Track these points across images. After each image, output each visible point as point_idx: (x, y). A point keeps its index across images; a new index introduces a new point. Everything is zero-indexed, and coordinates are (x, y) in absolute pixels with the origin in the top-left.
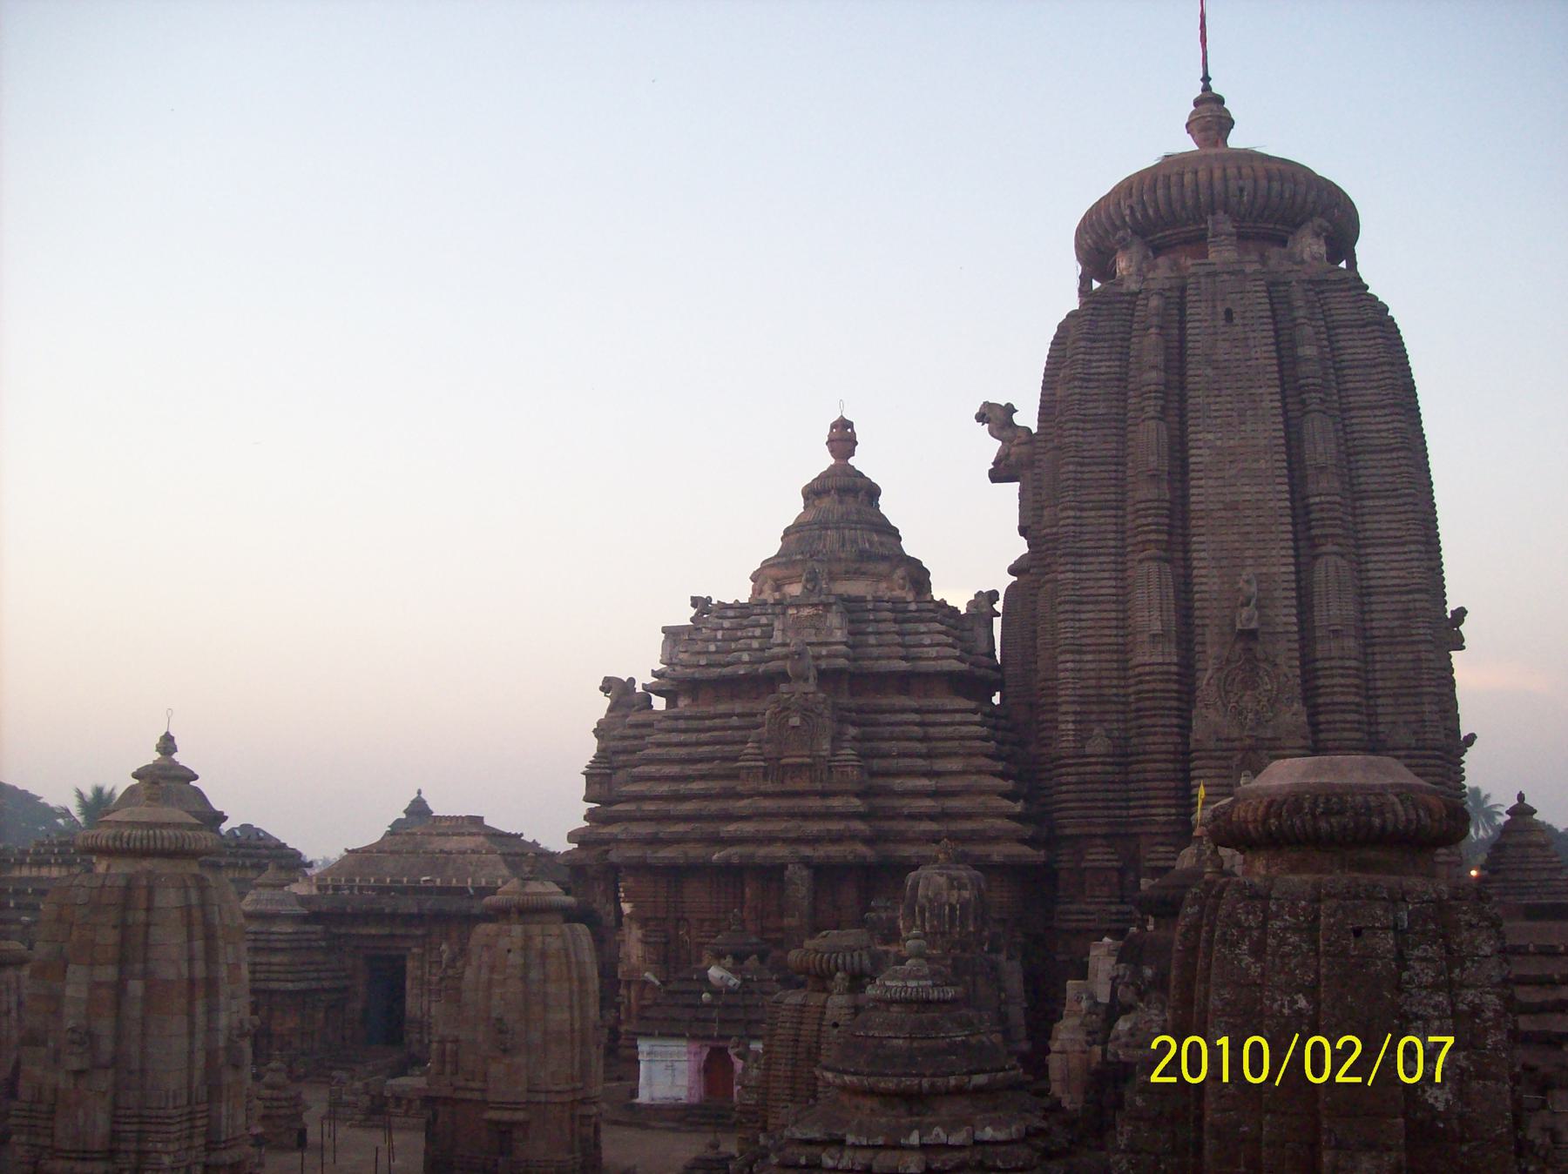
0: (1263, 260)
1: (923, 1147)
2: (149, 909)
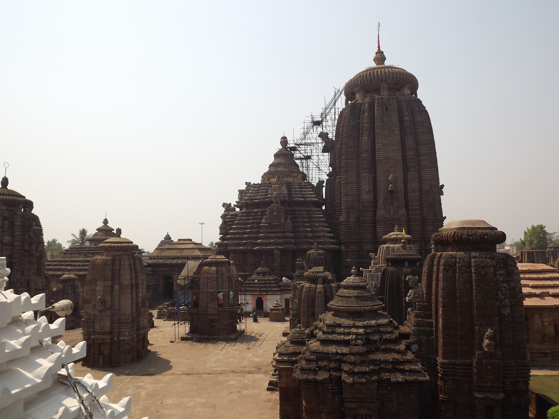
1: (363, 327)
2: (120, 265)
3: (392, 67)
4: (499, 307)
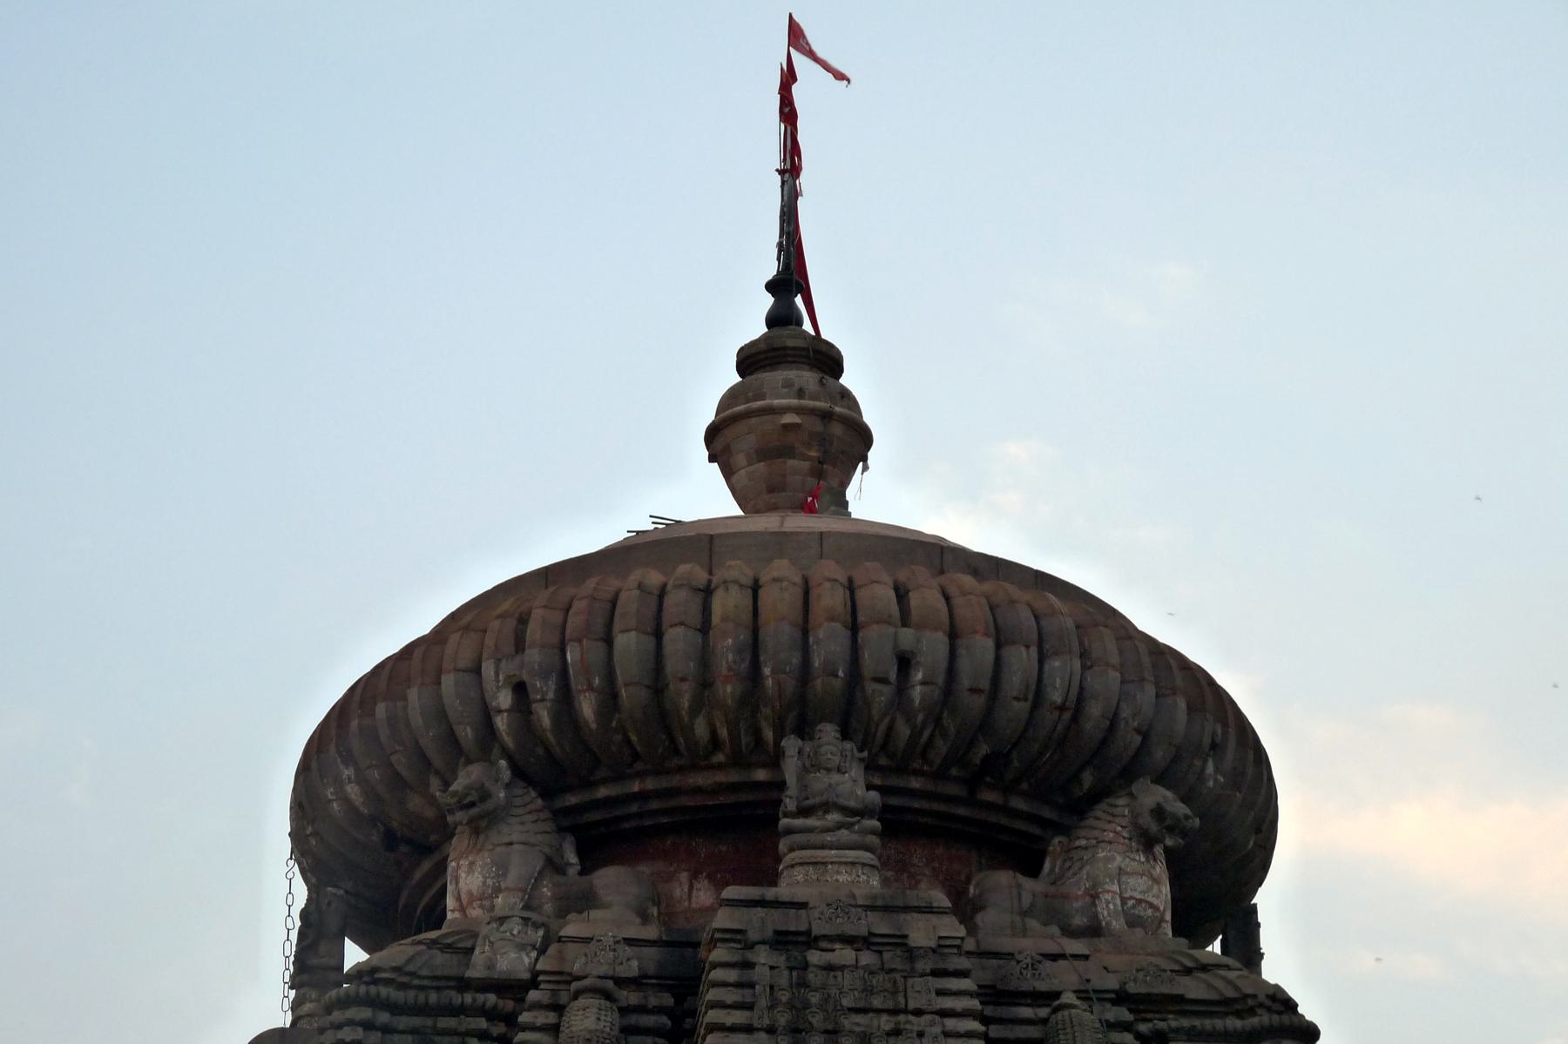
0: (965, 908)
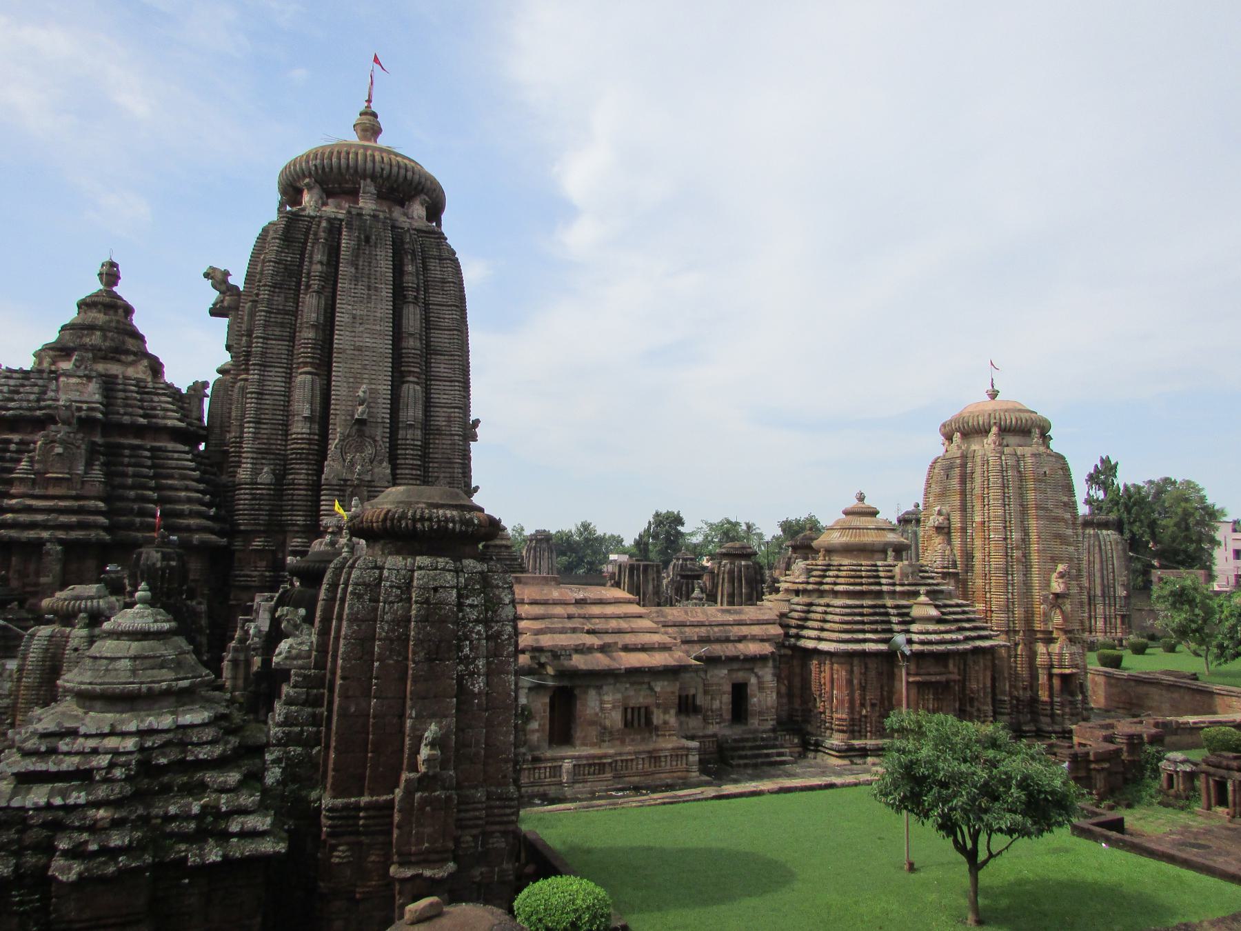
1: (140, 733)
3: (389, 152)
4: (460, 678)
